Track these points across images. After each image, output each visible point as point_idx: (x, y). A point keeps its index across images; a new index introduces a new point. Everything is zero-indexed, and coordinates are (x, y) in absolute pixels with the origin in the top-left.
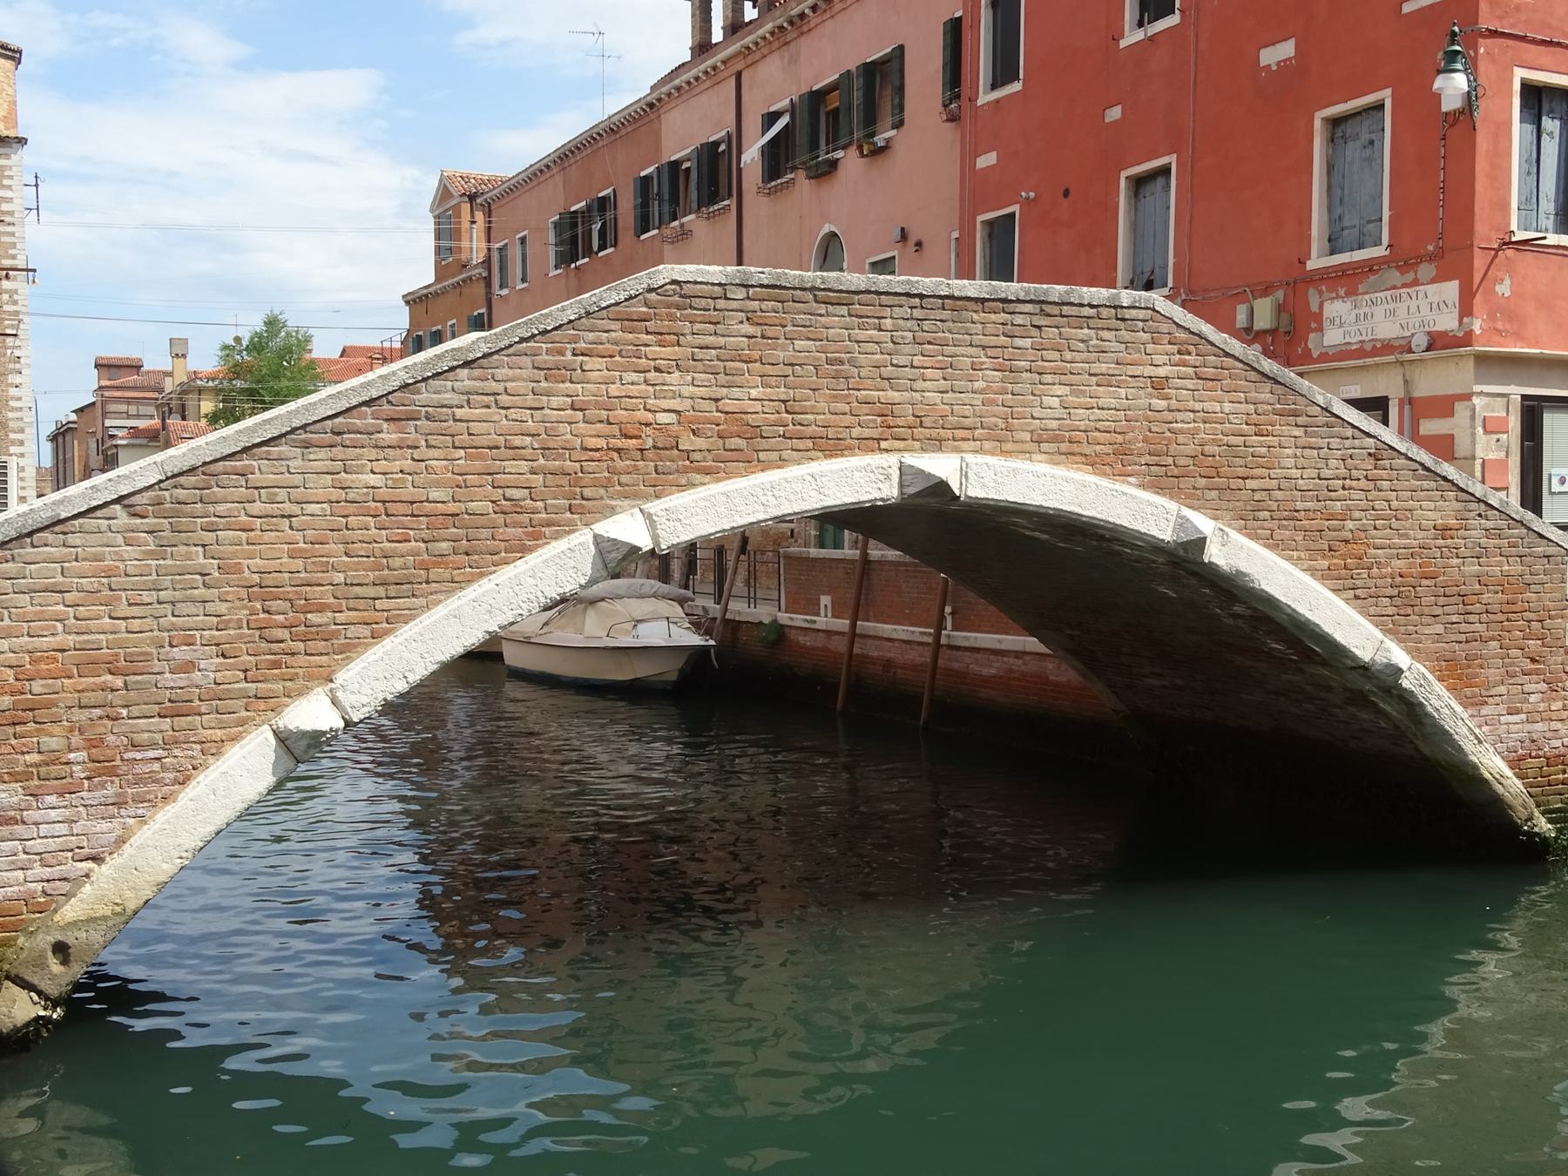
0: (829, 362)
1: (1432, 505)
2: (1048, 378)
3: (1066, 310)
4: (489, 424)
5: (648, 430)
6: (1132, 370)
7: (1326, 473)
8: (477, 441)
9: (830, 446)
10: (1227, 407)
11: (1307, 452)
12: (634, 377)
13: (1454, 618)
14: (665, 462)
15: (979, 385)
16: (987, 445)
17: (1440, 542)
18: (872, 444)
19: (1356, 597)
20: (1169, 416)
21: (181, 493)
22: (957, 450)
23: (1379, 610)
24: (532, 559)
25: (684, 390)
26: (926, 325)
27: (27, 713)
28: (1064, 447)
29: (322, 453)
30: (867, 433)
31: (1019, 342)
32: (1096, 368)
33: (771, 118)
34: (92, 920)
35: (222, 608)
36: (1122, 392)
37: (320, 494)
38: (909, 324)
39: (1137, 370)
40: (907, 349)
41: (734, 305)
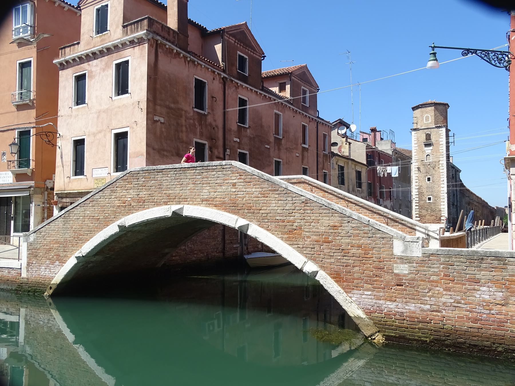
0: (159, 185)
1: (328, 218)
2: (205, 185)
3: (209, 168)
4: (103, 202)
7: (287, 208)
8: (102, 205)
9: (157, 204)
10: (254, 190)
11: (279, 202)
12: (125, 191)
13: (339, 258)
14: (129, 209)
15: (189, 188)
16: (191, 203)
17: (332, 231)
18: (166, 203)
19: (299, 247)
20: (236, 193)
25: (133, 193)
27: (50, 250)
28: (209, 202)
31: (198, 177)
32: (216, 182)
36: (224, 187)
40: (174, 181)
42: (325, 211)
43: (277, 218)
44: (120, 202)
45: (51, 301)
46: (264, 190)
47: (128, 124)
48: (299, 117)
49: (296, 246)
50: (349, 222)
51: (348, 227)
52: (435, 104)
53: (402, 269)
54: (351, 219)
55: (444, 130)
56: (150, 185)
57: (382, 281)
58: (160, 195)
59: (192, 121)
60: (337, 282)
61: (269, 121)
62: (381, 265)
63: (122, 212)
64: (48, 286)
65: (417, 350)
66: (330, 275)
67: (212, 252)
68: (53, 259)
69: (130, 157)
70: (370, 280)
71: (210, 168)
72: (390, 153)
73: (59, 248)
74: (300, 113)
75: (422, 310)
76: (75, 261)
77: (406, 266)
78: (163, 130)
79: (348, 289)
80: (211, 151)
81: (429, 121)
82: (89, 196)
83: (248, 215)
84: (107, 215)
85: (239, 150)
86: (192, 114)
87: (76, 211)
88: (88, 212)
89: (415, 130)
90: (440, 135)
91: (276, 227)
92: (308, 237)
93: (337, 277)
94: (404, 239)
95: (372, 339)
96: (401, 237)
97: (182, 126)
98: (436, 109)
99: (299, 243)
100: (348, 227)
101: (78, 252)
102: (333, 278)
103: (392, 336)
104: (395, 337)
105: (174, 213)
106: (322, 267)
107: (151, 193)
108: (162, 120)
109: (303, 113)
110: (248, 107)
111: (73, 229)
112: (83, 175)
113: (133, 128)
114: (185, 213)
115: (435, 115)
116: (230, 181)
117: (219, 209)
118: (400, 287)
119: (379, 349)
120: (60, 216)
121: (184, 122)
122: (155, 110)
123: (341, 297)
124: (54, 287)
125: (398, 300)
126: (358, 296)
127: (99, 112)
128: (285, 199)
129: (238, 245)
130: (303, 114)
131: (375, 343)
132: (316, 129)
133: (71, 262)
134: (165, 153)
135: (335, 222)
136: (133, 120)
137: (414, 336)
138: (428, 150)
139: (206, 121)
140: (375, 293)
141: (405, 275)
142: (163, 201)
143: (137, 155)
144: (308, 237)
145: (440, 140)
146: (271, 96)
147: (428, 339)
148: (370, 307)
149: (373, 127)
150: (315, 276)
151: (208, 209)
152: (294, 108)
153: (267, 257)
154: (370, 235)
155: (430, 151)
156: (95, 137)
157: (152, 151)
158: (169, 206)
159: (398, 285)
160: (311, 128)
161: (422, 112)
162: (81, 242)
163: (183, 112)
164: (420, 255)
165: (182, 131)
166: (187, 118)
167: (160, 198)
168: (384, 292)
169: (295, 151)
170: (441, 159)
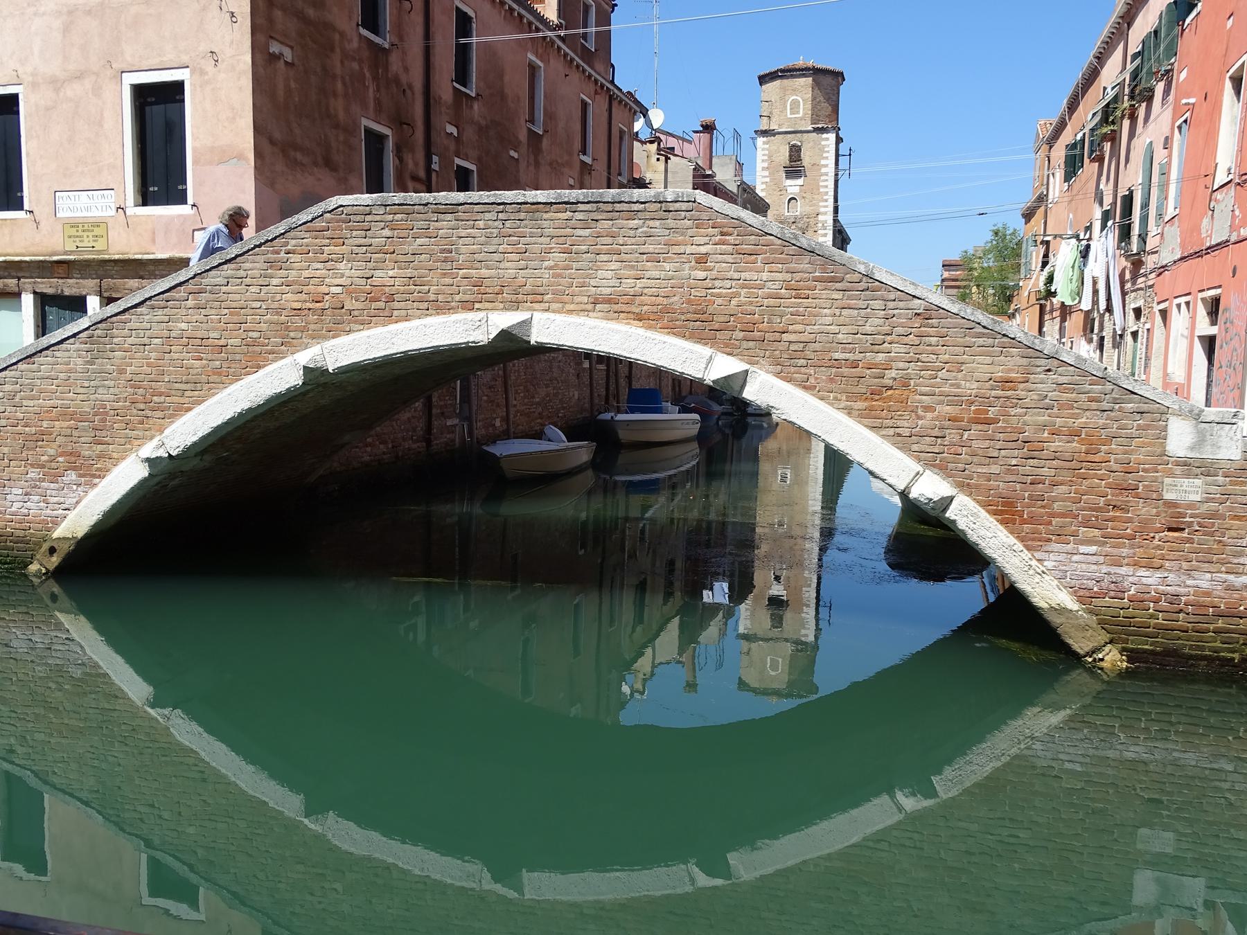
0: (443, 251)
1: (988, 360)
2: (605, 258)
4: (236, 294)
5: (327, 297)
6: (677, 249)
7: (868, 329)
8: (234, 305)
9: (440, 307)
10: (765, 276)
11: (845, 312)
12: (320, 266)
13: (1014, 462)
14: (339, 319)
15: (551, 263)
16: (554, 306)
17: (1000, 393)
18: (468, 306)
19: (899, 435)
20: (708, 283)
21: (99, 332)
22: (529, 309)
23: (923, 448)
24: (261, 372)
25: (348, 272)
26: (508, 224)
28: (616, 307)
29: (160, 312)
30: (467, 297)
32: (643, 249)
33: (1135, 56)
34: (64, 538)
35: (116, 391)
36: (667, 266)
38: (496, 223)
39: (680, 249)
40: (496, 241)
41: (378, 218)
42: (981, 341)
43: (836, 356)
44: (303, 296)
45: (56, 589)
46: (798, 276)
47: (185, 59)
48: (575, 77)
49: (891, 432)
50: (1049, 370)
51: (1045, 384)
52: (816, 72)
53: (1187, 490)
54: (1056, 362)
55: (832, 137)
56: (410, 249)
57: (1130, 520)
58: (447, 280)
59: (355, 66)
60: (1003, 522)
61: (516, 84)
62: (1131, 480)
63: (312, 327)
64: (39, 545)
65: (1208, 679)
66: (985, 505)
67: (404, 439)
69: (195, 162)
70: (1097, 517)
71: (625, 207)
72: (735, 190)
73: (75, 433)
74: (578, 66)
75: (1230, 588)
76: (143, 472)
77: (1198, 482)
78: (293, 85)
79: (1033, 540)
80: (401, 159)
81: (798, 112)
82: (182, 275)
83: (745, 344)
84: (255, 335)
85: (458, 161)
86: (355, 44)
87: (133, 320)
88: (184, 326)
89: (765, 133)
90: (822, 150)
92: (928, 409)
93: (1006, 512)
94: (1199, 415)
95: (1095, 660)
96: (1191, 412)
97: (334, 77)
98: (817, 84)
99: (899, 423)
100: (1045, 384)
101: (155, 442)
102: (994, 513)
103: (1145, 651)
104: (1153, 653)
105: (505, 335)
106: (965, 487)
107: (416, 273)
108: (288, 55)
109: (586, 67)
110: (474, 40)
111: (129, 377)
112: (21, 208)
113: (202, 72)
114: (538, 335)
115: (814, 99)
116: (689, 249)
117: (649, 328)
118: (1176, 534)
119: (1108, 683)
120: (74, 335)
121: (338, 64)
122: (271, 20)
123: (1016, 561)
124: (65, 548)
125: (1167, 564)
126: (1062, 557)
127: (70, 13)
128: (862, 304)
129: (456, 421)
130: (584, 71)
131: (1102, 669)
132: (606, 114)
133: (125, 476)
134: (299, 156)
135: (1010, 371)
136: (204, 47)
137: (1202, 648)
138: (793, 186)
139: (386, 69)
140: (1107, 549)
141: (1192, 505)
142: (457, 298)
143: (224, 156)
144: (928, 409)
145: (823, 162)
146: (523, 12)
147: (1236, 656)
148: (1091, 584)
149: (708, 118)
150: (945, 509)
151: (613, 325)
152: (567, 50)
153: (550, 451)
154: (1105, 405)
155: (797, 189)
156: (57, 90)
157: (267, 148)
158: (481, 314)
159: (1170, 529)
160: (597, 108)
161: (784, 89)
162: (159, 414)
163: (337, 37)
164: (1236, 454)
165: (335, 95)
166: (346, 56)
167: (448, 290)
168: (1132, 546)
169: (566, 170)
170: (822, 210)
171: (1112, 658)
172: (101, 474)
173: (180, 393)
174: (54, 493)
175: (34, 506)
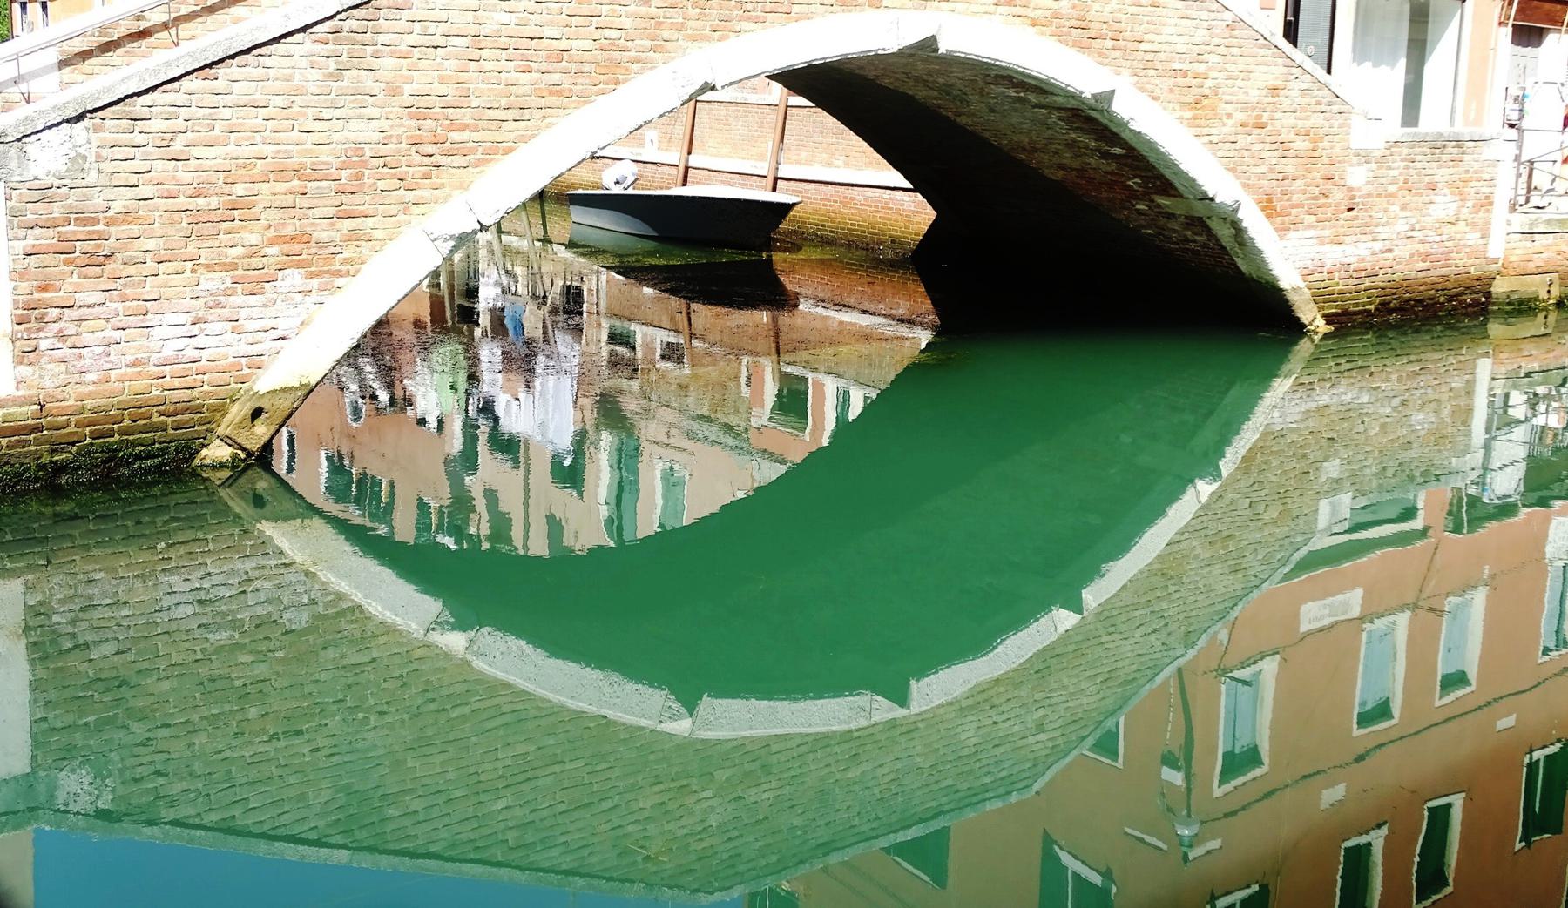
7: (1196, 40)
35: (384, 124)
37: (463, 30)
49: (1206, 139)
64: (221, 410)
68: (256, 262)
73: (303, 202)
84: (614, 34)
91: (1171, 91)
92: (1229, 116)
99: (1213, 131)
144: (1229, 116)
162: (459, 161)
171: (1322, 326)
172: (351, 269)
173: (494, 125)
174: (256, 313)
175: (218, 346)
